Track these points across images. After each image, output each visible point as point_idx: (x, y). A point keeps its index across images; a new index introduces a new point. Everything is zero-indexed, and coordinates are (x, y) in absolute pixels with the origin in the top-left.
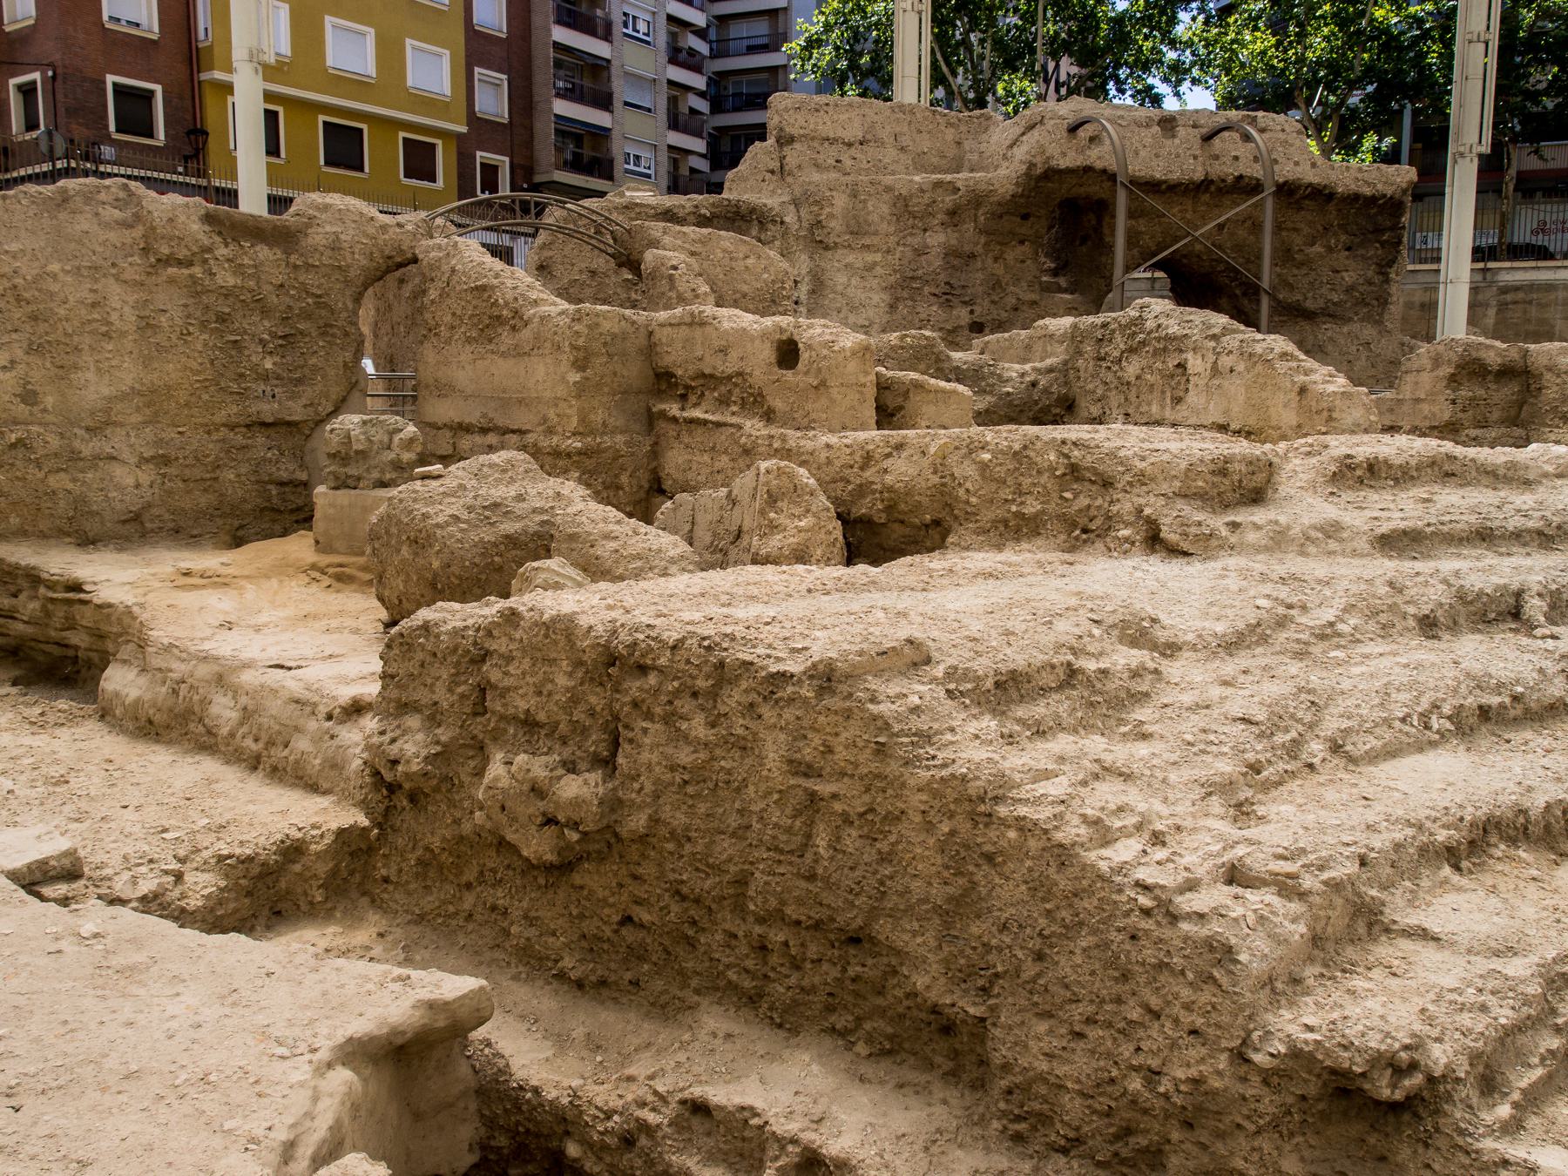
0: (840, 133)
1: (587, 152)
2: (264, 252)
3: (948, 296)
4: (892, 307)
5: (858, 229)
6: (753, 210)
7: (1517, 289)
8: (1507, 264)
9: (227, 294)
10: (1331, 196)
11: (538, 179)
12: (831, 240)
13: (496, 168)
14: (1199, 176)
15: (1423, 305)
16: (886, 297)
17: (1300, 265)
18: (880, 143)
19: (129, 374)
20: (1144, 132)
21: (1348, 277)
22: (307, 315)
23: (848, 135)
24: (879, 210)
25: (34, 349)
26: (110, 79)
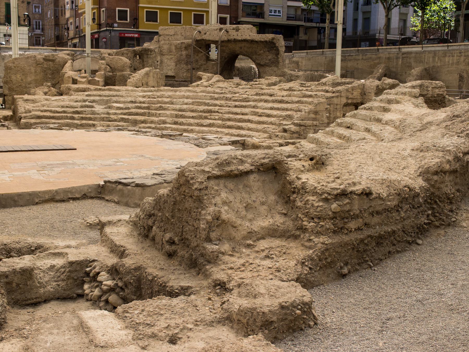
0: (169, 34)
1: (258, 11)
2: (50, 63)
3: (187, 64)
4: (176, 66)
5: (170, 51)
6: (149, 49)
7: (405, 53)
8: (394, 47)
9: (46, 68)
10: (256, 42)
11: (239, 20)
12: (164, 53)
13: (226, 18)
14: (226, 39)
15: (388, 58)
16: (175, 64)
17: (259, 55)
18: (177, 35)
19: (33, 78)
20: (216, 32)
21: (269, 57)
22: (55, 70)
23: (171, 34)
24: (173, 48)
25: (23, 75)
26: (117, 9)
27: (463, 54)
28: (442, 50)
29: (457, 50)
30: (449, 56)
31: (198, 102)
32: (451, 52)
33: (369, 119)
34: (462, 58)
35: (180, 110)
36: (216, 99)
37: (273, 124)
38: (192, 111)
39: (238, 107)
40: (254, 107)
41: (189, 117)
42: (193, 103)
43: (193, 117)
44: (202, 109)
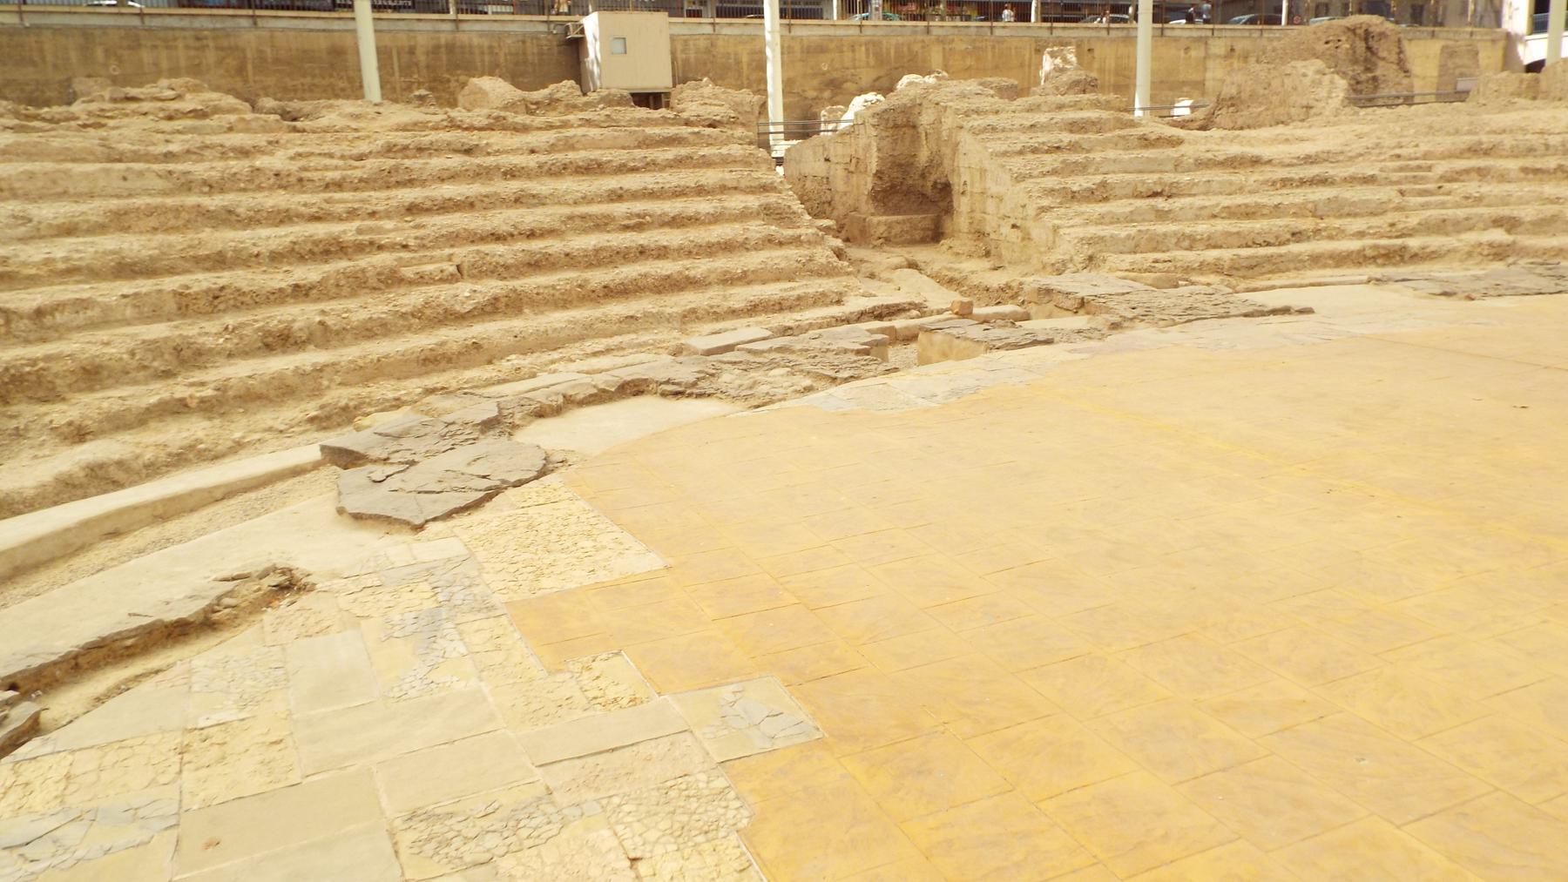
27: (211, 44)
28: (119, 28)
29: (183, 29)
30: (155, 47)
31: (151, 212)
32: (162, 34)
33: (1170, 166)
34: (211, 56)
35: (125, 269)
36: (211, 187)
37: (781, 244)
38: (219, 261)
39: (428, 210)
40: (518, 201)
41: (278, 297)
42: (119, 221)
43: (300, 292)
44: (274, 245)
